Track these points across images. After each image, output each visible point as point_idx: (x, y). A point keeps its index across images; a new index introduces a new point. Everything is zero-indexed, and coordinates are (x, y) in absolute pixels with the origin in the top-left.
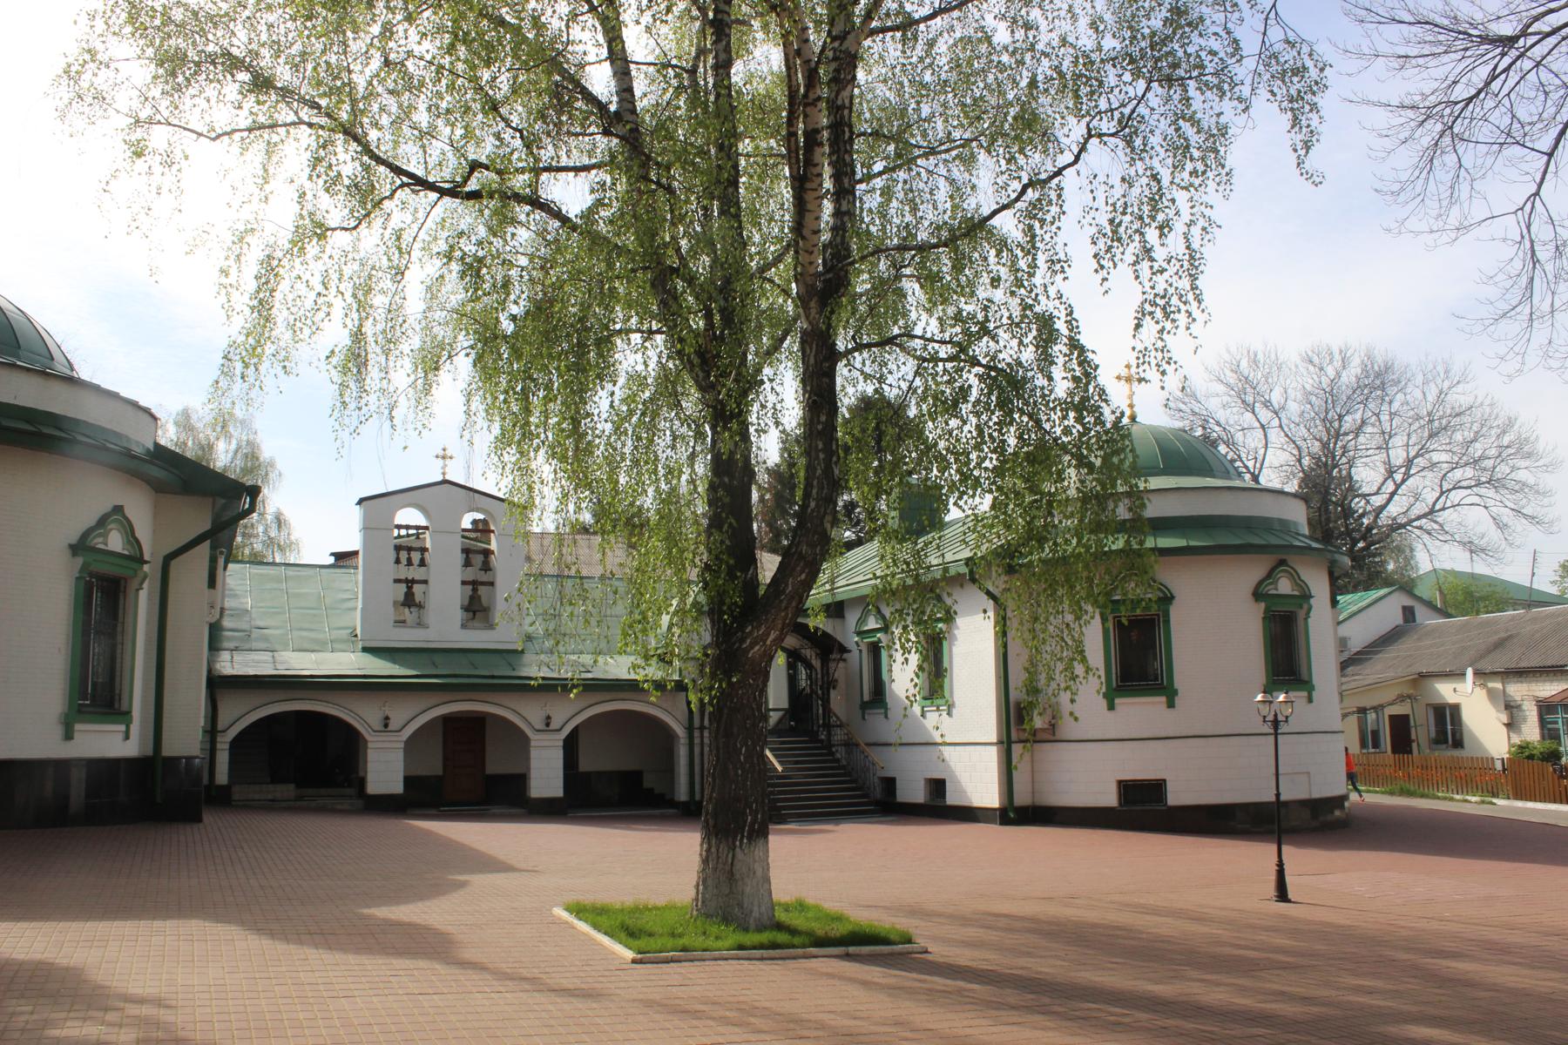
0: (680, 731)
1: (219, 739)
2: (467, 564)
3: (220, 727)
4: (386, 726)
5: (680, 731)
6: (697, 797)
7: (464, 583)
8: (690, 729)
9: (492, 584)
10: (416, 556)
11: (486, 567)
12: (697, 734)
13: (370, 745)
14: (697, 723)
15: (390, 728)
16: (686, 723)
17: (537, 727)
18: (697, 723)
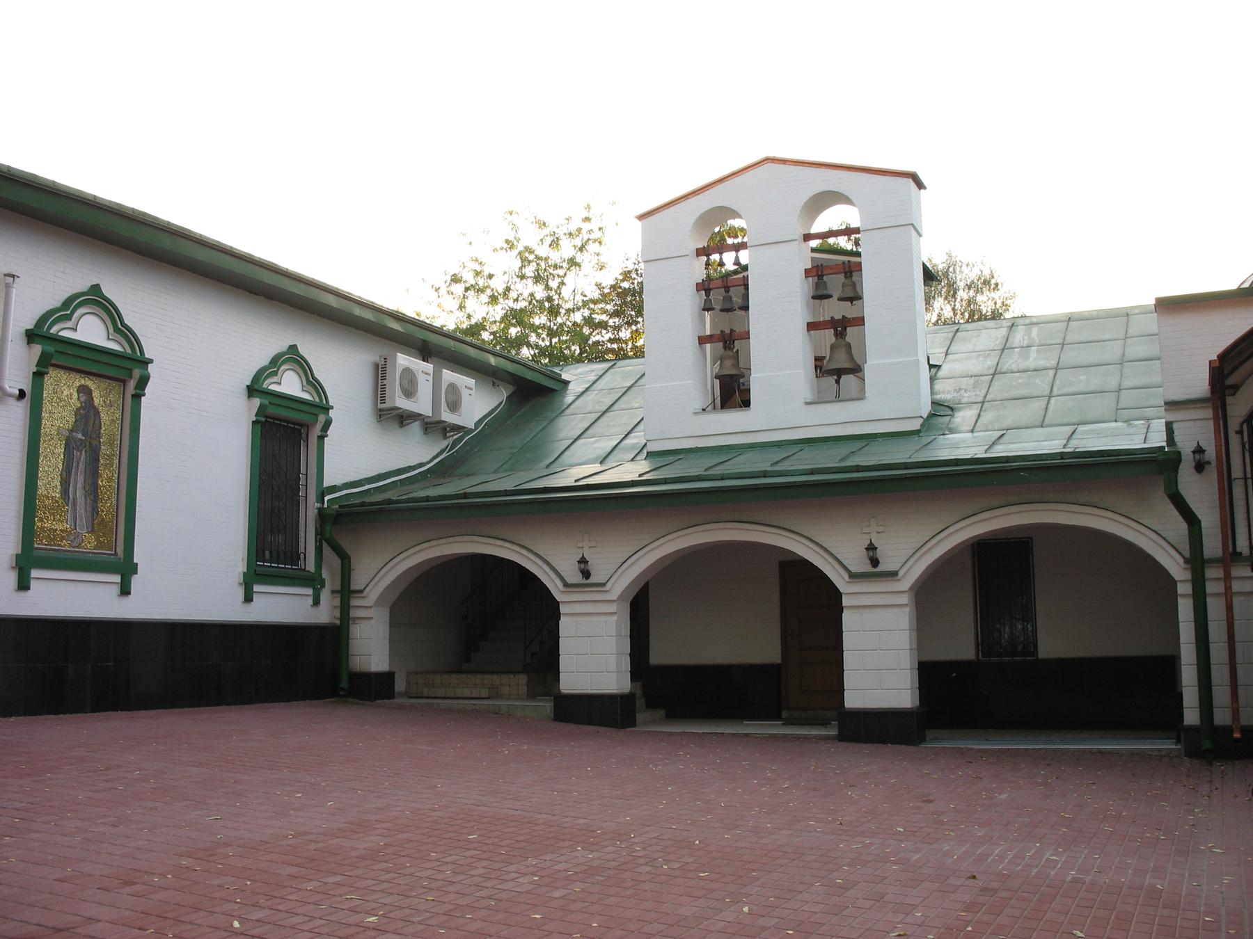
0: (1175, 566)
1: (354, 602)
2: (820, 295)
3: (357, 584)
4: (586, 574)
5: (1175, 566)
6: (1222, 717)
7: (811, 326)
8: (1196, 561)
9: (860, 321)
10: (736, 293)
11: (854, 297)
12: (1212, 573)
13: (563, 609)
14: (1212, 545)
15: (592, 580)
16: (1186, 549)
17: (854, 569)
18: (1212, 545)
